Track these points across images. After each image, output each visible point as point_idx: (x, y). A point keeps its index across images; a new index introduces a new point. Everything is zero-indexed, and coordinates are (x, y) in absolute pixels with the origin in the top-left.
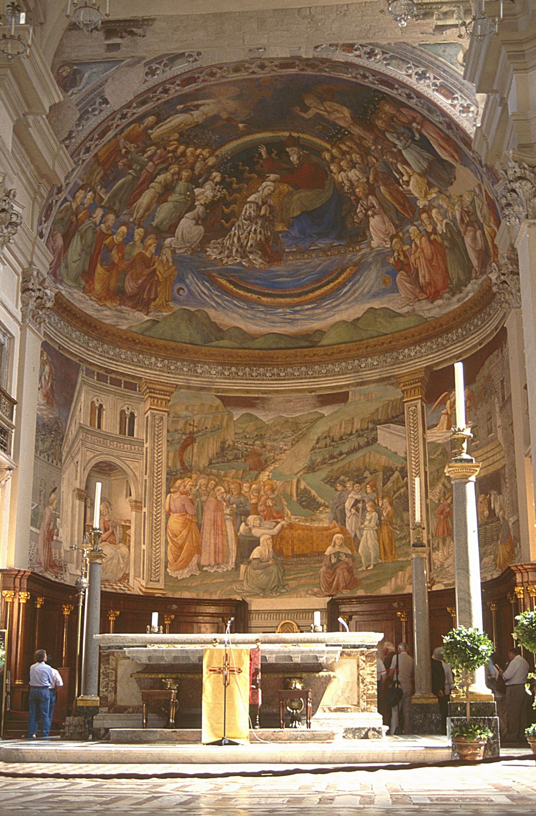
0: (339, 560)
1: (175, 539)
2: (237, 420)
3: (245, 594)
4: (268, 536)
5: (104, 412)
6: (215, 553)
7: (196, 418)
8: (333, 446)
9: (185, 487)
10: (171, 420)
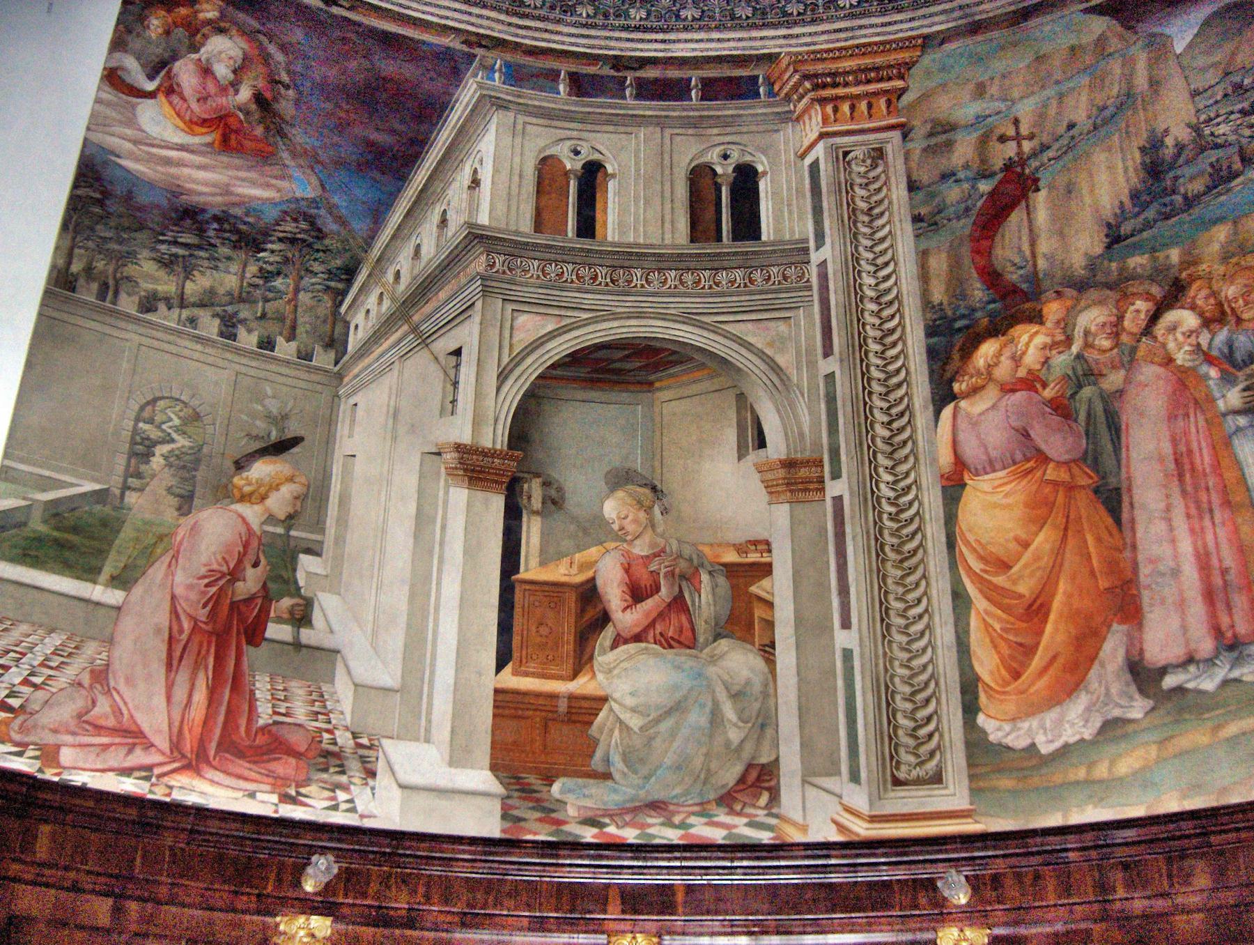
1: (1000, 580)
2: (1190, 46)
5: (612, 185)
6: (1209, 596)
7: (1026, 110)
9: (1017, 360)
10: (917, 145)
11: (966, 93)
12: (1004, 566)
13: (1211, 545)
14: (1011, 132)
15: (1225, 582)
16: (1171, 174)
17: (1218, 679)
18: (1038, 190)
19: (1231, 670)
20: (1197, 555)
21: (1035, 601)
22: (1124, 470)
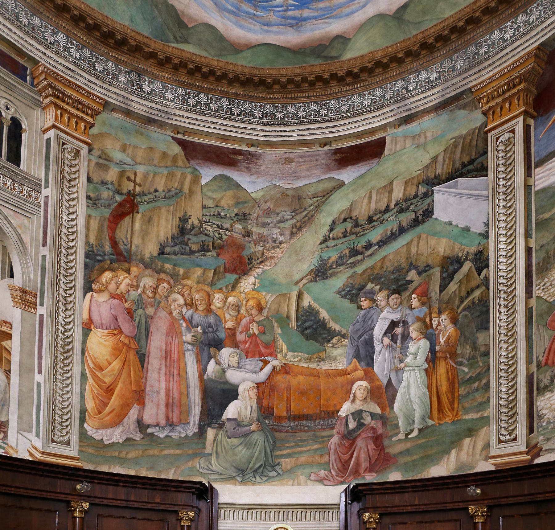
0: (360, 425)
3: (214, 477)
6: (167, 405)
8: (357, 234)
11: (118, 145)
12: (101, 369)
15: (173, 402)
16: (187, 236)
17: (165, 434)
18: (138, 212)
20: (166, 389)
21: (109, 386)
22: (148, 349)
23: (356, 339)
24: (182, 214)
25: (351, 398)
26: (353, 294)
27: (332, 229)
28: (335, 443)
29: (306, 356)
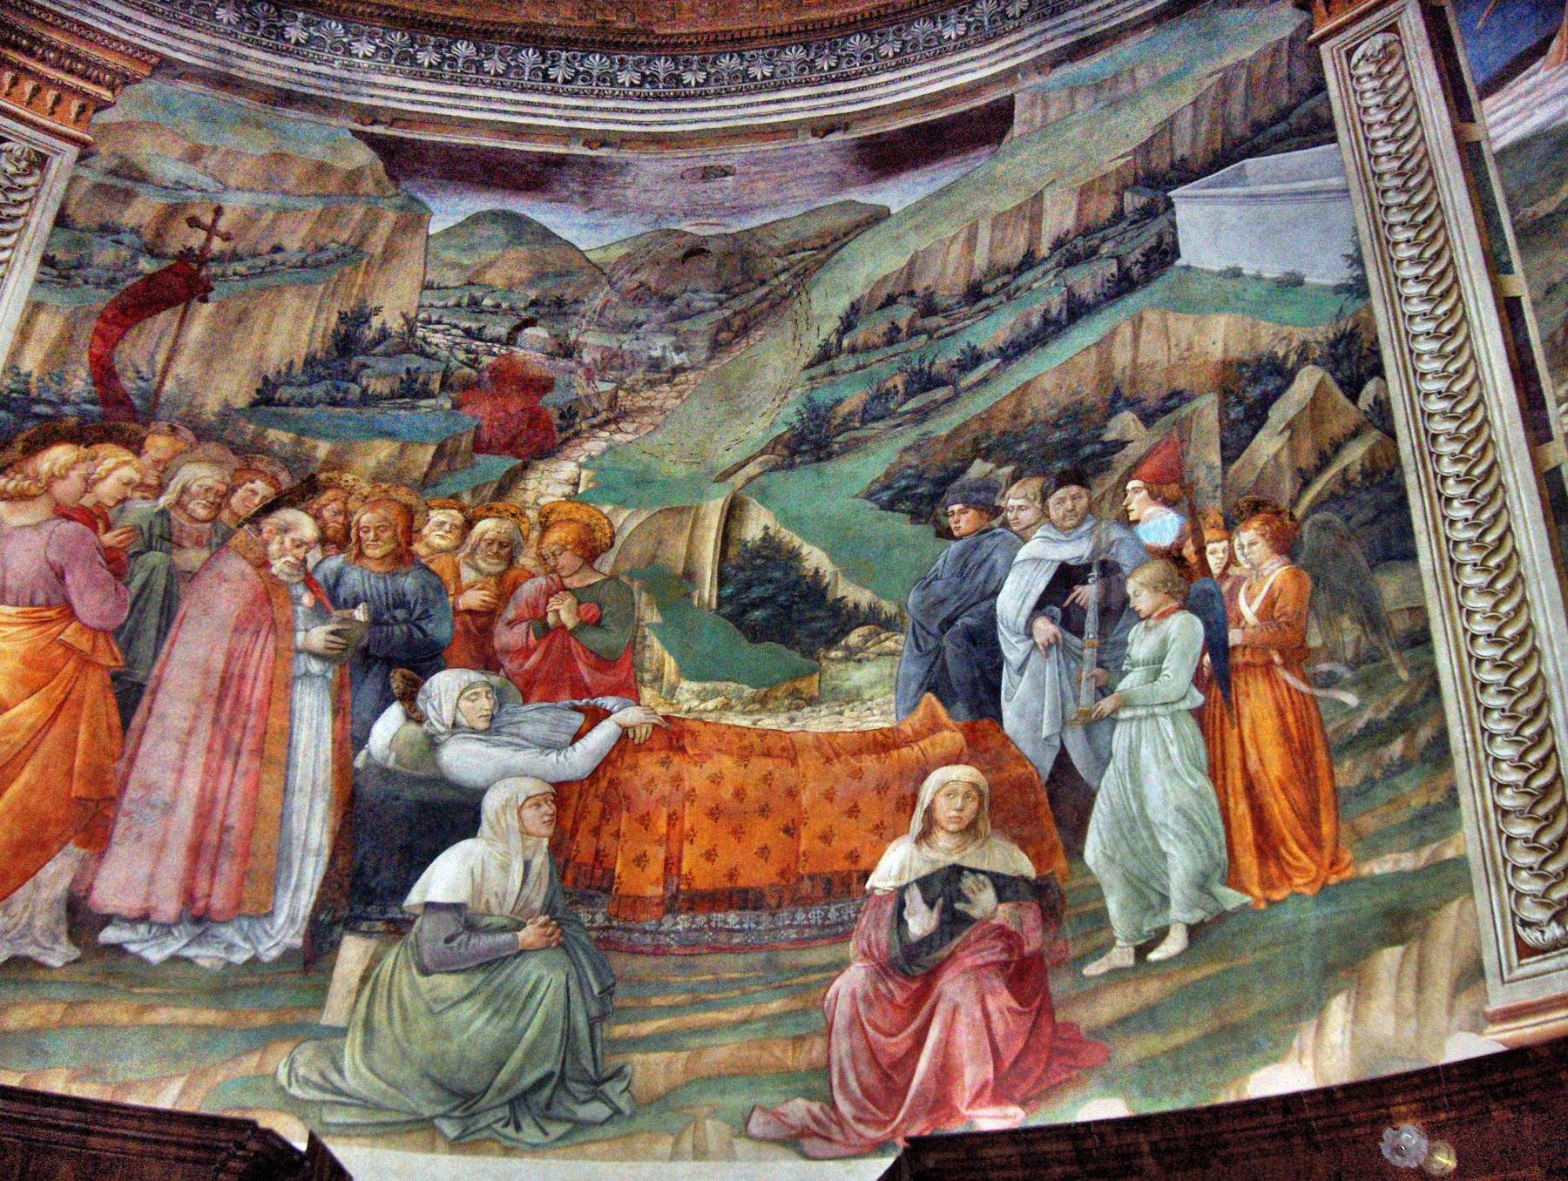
0: (954, 921)
2: (448, 232)
4: (531, 787)
6: (196, 851)
7: (236, 204)
9: (89, 484)
11: (177, 149)
13: (222, 795)
14: (207, 219)
15: (221, 840)
16: (361, 359)
17: (168, 952)
18: (205, 300)
19: (187, 945)
20: (201, 797)
22: (158, 665)
23: (934, 629)
24: (352, 303)
25: (916, 824)
26: (922, 496)
27: (848, 325)
28: (853, 996)
29: (748, 691)
